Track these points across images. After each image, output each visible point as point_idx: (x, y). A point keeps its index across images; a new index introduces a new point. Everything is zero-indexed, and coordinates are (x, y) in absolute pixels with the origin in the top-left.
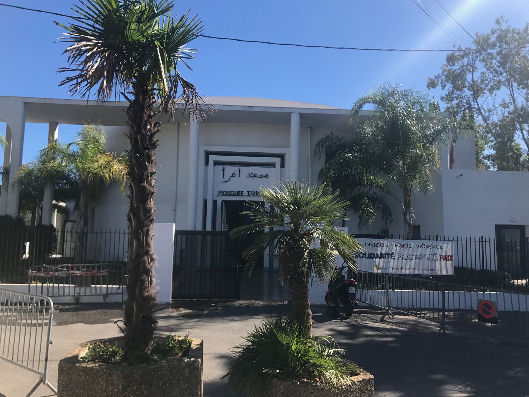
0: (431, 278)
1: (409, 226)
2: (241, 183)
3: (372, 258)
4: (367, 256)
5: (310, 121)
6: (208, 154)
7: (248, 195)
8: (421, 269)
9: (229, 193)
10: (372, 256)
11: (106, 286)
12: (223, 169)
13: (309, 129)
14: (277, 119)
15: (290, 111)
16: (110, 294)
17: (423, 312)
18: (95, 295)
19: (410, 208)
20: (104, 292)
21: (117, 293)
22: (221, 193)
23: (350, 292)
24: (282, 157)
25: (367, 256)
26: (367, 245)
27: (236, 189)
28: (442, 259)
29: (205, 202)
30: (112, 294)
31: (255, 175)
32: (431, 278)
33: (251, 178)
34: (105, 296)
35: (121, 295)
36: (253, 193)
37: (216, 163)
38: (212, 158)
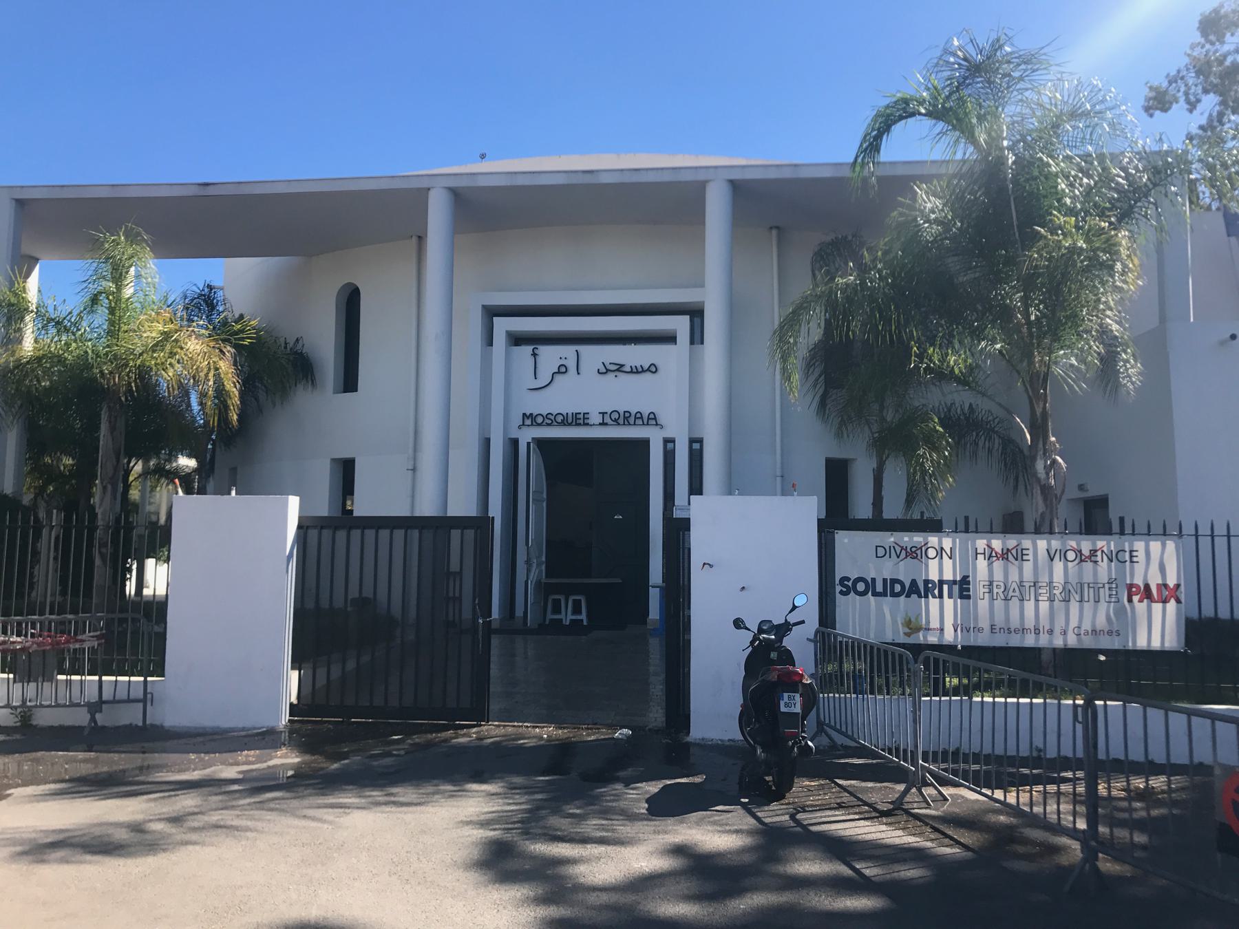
0: (1102, 658)
1: (1043, 492)
2: (588, 393)
3: (894, 595)
4: (879, 588)
5: (773, 208)
6: (491, 312)
7: (603, 424)
8: (1057, 630)
9: (550, 420)
10: (898, 588)
11: (142, 679)
12: (534, 355)
13: (774, 232)
14: (665, 207)
15: (701, 177)
16: (105, 702)
17: (1069, 775)
18: (65, 706)
19: (1046, 438)
20: (91, 695)
21: (129, 701)
22: (530, 419)
23: (783, 709)
24: (696, 314)
25: (879, 588)
26: (881, 552)
27: (568, 408)
28: (1136, 598)
29: (486, 443)
30: (115, 701)
31: (620, 368)
32: (1102, 658)
33: (611, 376)
34: (95, 707)
35: (141, 705)
36: (615, 416)
37: (517, 340)
38: (502, 325)
